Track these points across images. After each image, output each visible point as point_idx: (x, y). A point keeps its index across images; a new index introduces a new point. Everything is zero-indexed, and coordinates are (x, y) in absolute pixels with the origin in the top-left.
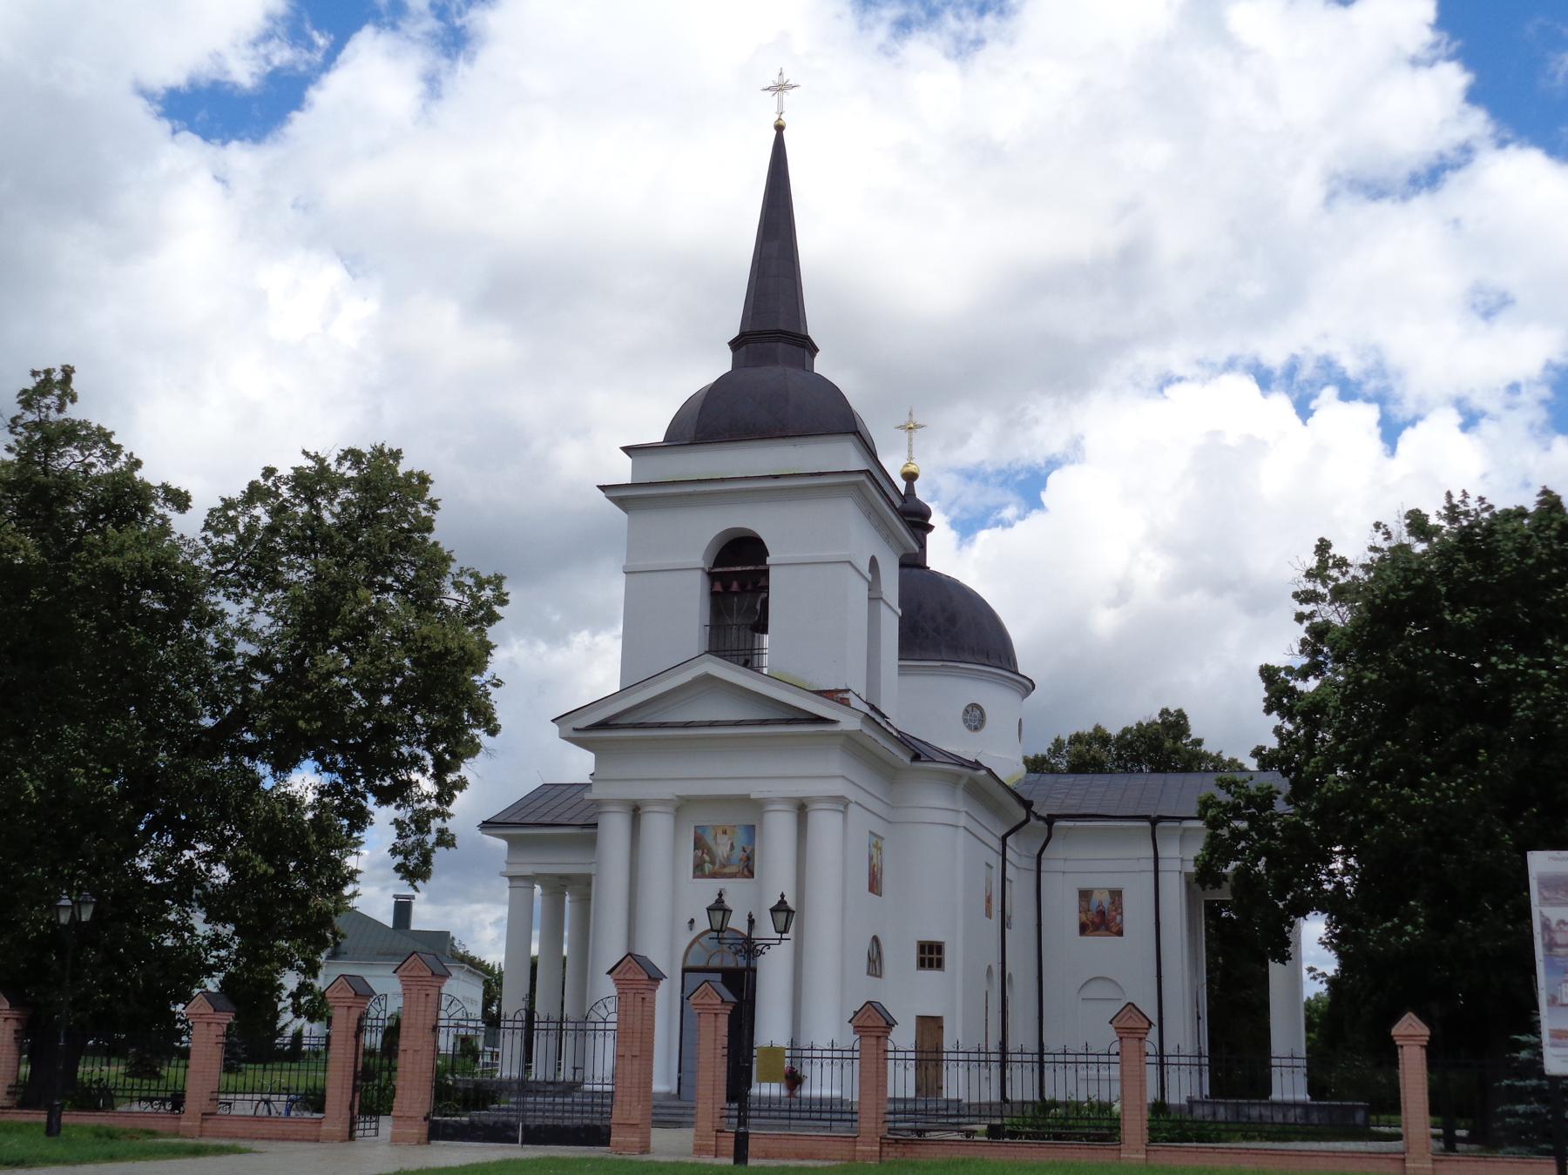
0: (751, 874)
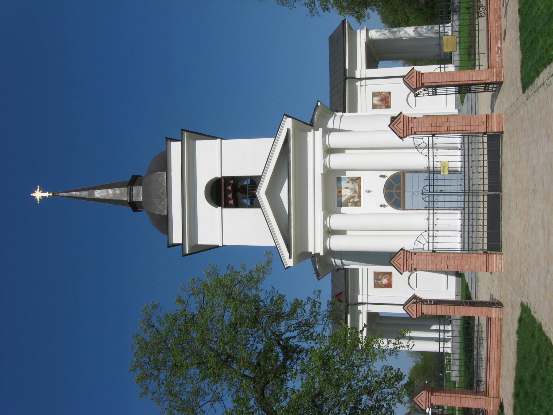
0: (359, 178)
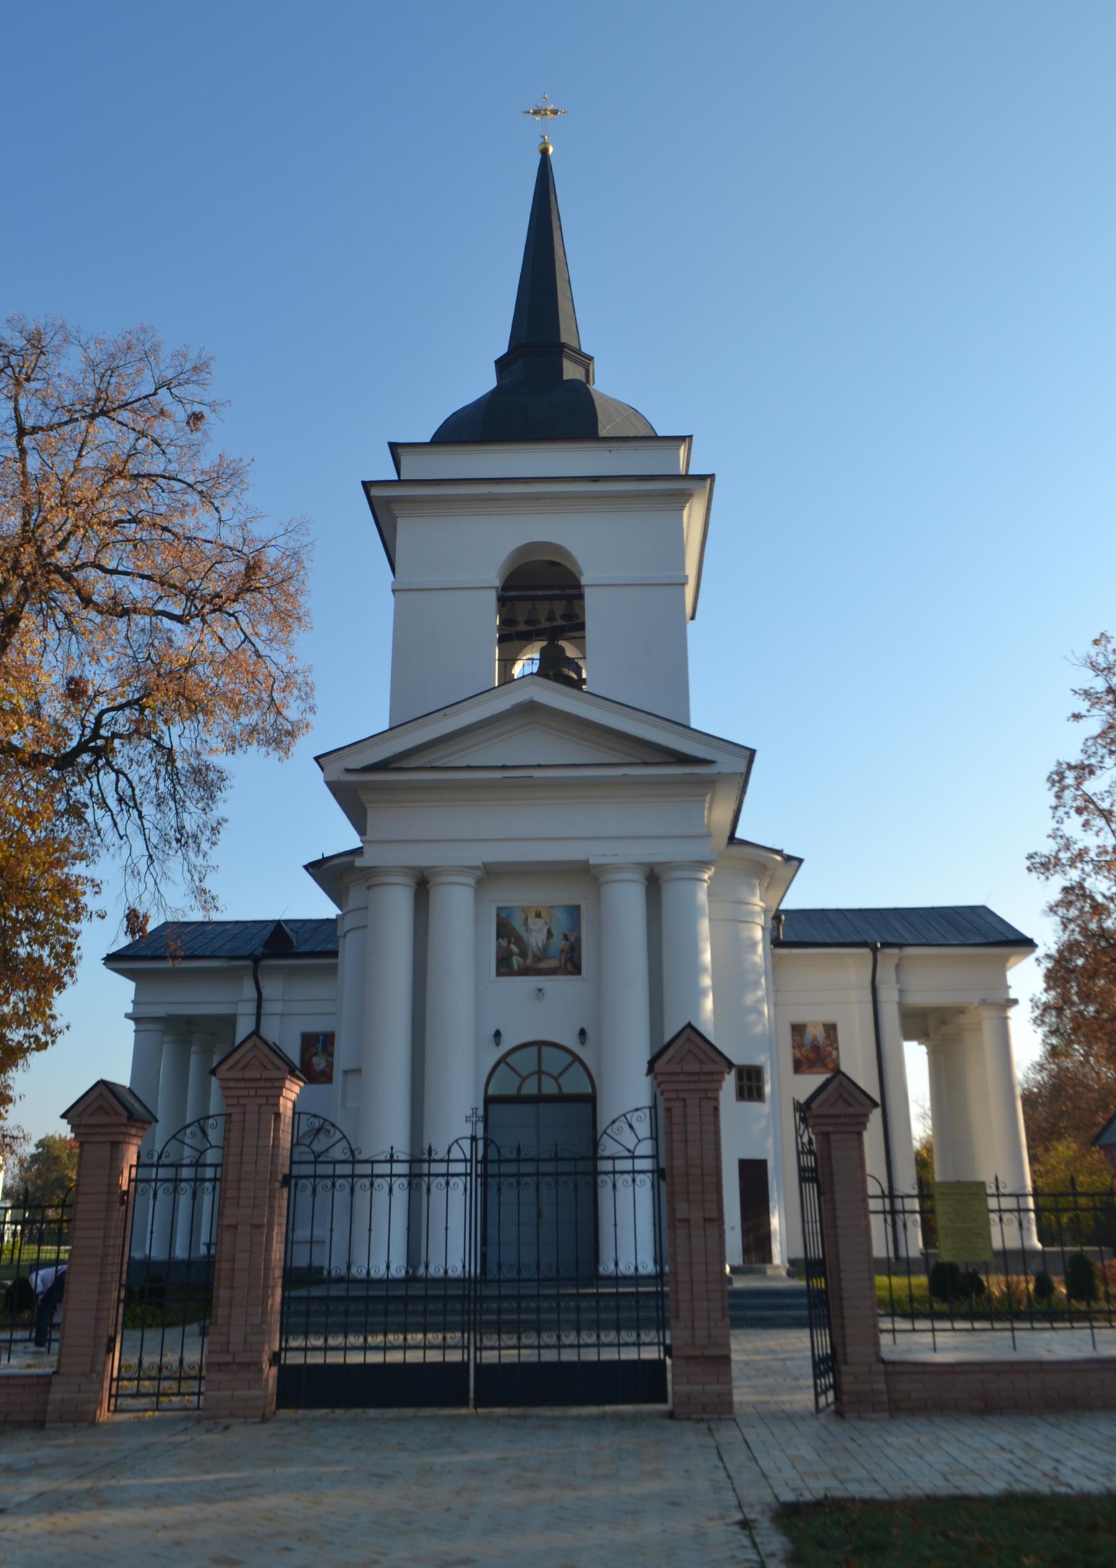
0: (577, 970)
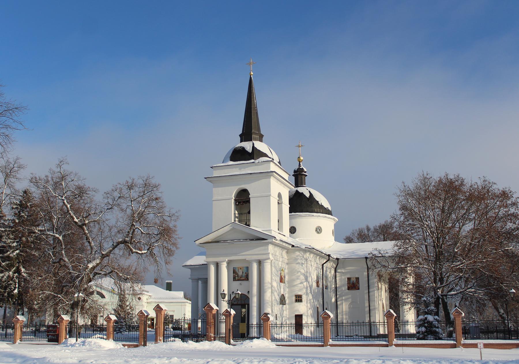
0: (248, 280)
